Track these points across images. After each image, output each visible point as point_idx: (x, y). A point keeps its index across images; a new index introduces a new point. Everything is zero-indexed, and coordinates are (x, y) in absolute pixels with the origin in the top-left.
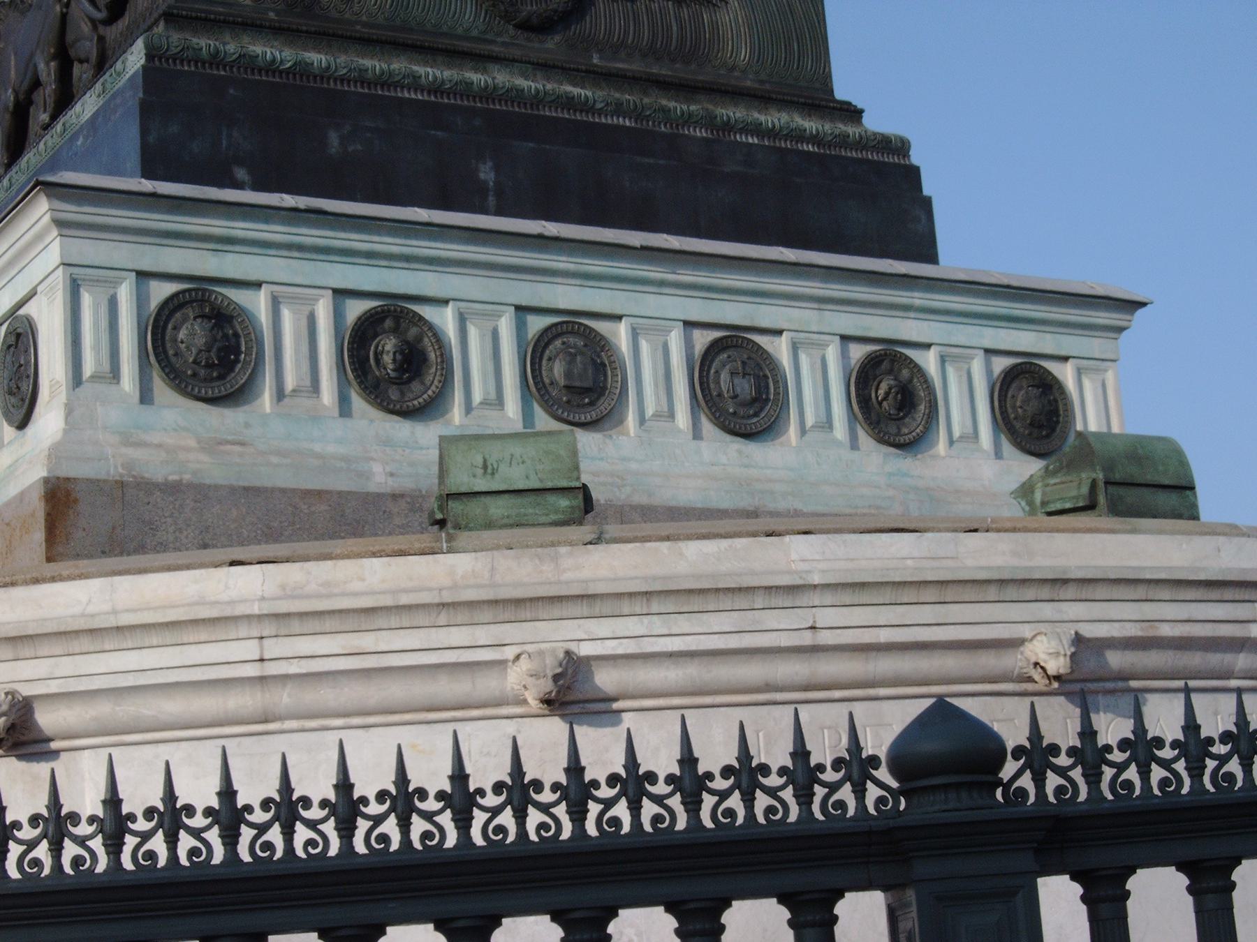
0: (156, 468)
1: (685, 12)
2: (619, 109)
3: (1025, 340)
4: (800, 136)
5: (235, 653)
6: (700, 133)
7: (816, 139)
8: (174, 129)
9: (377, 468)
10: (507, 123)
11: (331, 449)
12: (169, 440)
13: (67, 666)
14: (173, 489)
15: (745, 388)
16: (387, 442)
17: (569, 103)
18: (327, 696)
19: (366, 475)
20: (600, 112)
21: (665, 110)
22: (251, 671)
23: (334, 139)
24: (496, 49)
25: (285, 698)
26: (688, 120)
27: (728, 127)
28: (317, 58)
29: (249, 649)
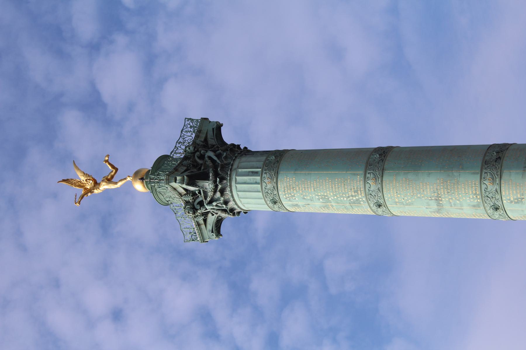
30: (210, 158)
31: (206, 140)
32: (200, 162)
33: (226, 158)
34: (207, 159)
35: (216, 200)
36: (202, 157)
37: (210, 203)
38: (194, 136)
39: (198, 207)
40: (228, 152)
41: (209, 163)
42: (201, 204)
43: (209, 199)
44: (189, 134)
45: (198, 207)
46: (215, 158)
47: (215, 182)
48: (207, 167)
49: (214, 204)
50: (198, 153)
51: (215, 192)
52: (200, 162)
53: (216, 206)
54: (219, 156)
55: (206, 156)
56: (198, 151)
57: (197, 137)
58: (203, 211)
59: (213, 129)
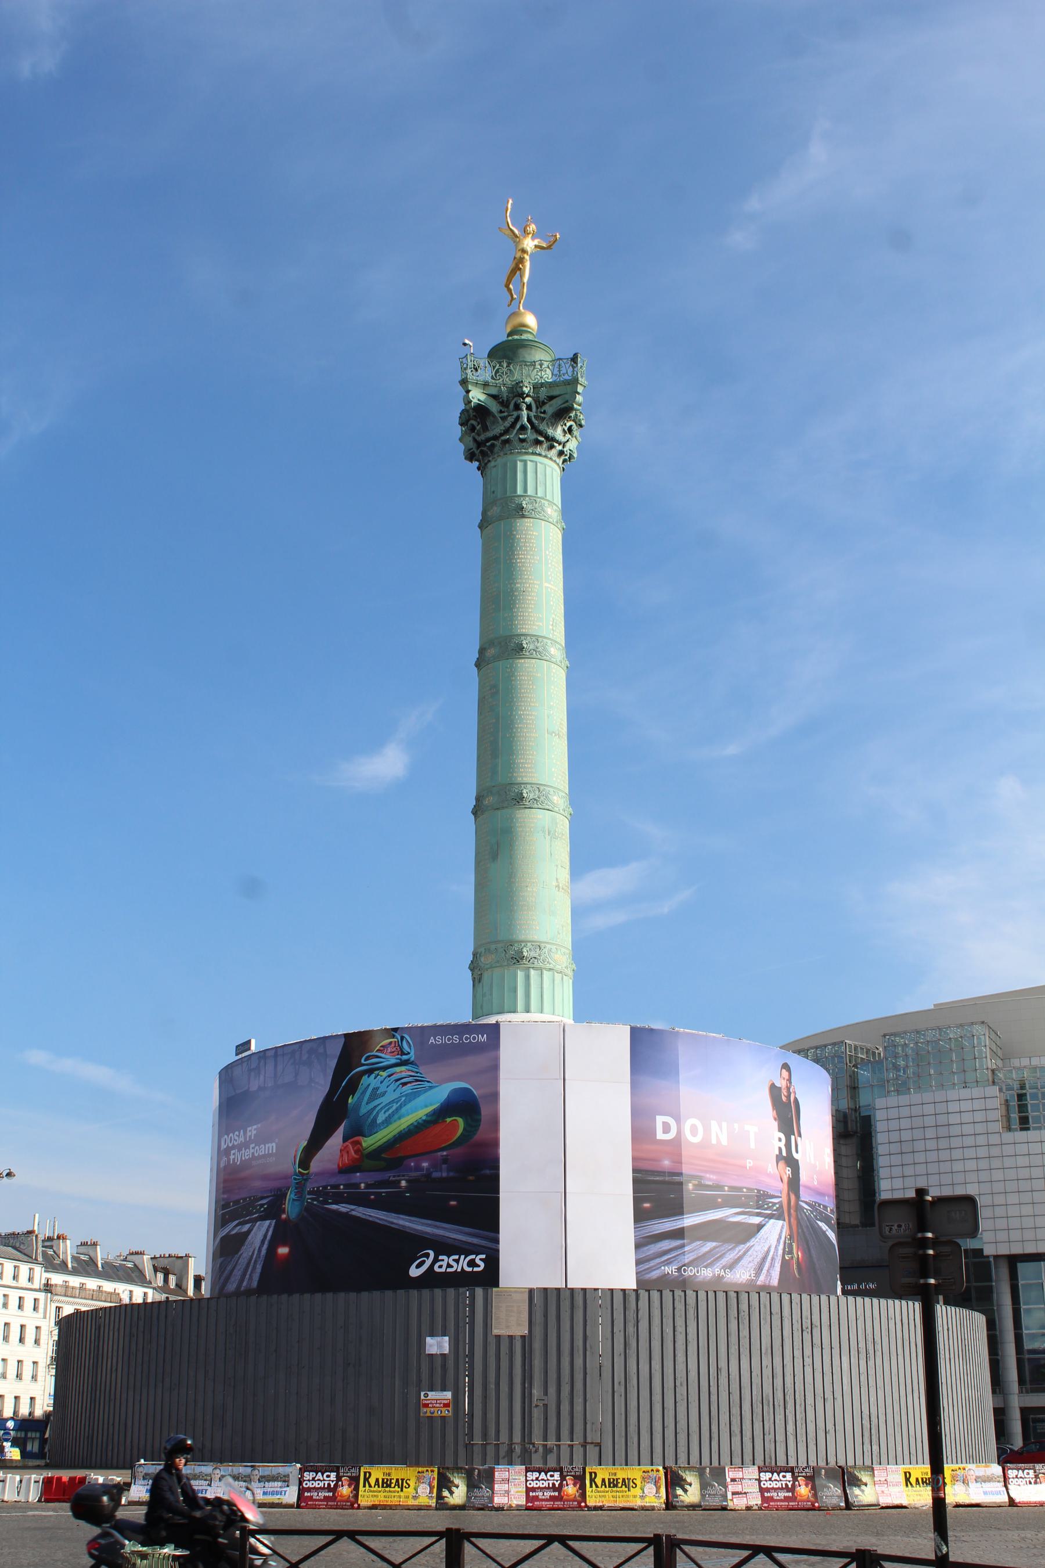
30: (518, 418)
31: (551, 398)
32: (512, 406)
33: (522, 441)
34: (515, 414)
36: (517, 407)
37: (475, 440)
38: (555, 378)
41: (510, 420)
42: (473, 429)
44: (556, 372)
46: (518, 426)
47: (488, 440)
48: (504, 419)
52: (512, 406)
57: (550, 385)
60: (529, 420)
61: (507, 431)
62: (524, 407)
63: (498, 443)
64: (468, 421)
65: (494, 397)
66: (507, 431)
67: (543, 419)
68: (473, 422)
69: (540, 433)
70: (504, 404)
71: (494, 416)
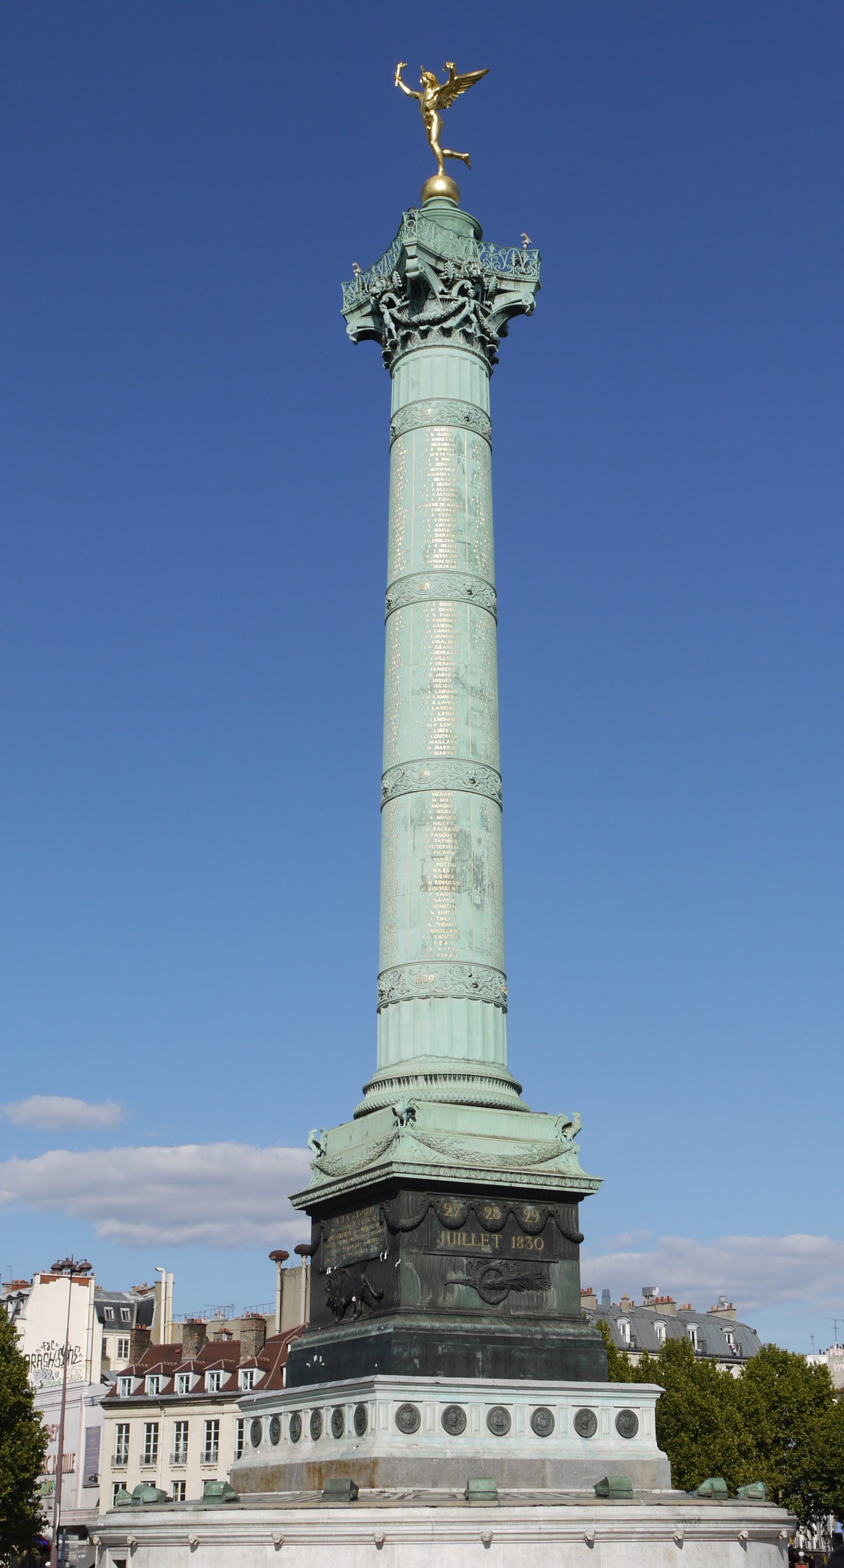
0: (397, 1454)
1: (539, 1293)
2: (517, 1332)
3: (626, 1403)
4: (568, 1334)
5: (428, 1528)
6: (539, 1337)
7: (572, 1335)
8: (400, 1350)
9: (449, 1451)
10: (486, 1339)
11: (437, 1445)
12: (399, 1445)
13: (395, 1528)
14: (400, 1459)
15: (544, 1423)
16: (451, 1443)
17: (503, 1331)
18: (445, 1537)
19: (445, 1454)
20: (512, 1333)
21: (529, 1331)
22: (430, 1532)
23: (440, 1349)
24: (484, 1312)
25: (436, 1537)
26: (537, 1333)
27: (547, 1334)
28: (437, 1325)
29: (430, 1528)
30: (463, 306)
34: (462, 299)
35: (397, 329)
36: (463, 292)
39: (385, 298)
40: (479, 334)
41: (453, 305)
42: (391, 304)
43: (398, 315)
45: (385, 298)
49: (392, 326)
50: (468, 284)
51: (407, 325)
53: (390, 331)
54: (467, 320)
55: (466, 299)
56: (473, 283)
58: (383, 308)
59: (520, 301)
60: (475, 312)
61: (445, 318)
62: (471, 292)
63: (436, 328)
64: (383, 293)
65: (438, 272)
66: (445, 318)
67: (486, 314)
68: (392, 296)
69: (483, 330)
70: (448, 283)
71: (435, 298)
